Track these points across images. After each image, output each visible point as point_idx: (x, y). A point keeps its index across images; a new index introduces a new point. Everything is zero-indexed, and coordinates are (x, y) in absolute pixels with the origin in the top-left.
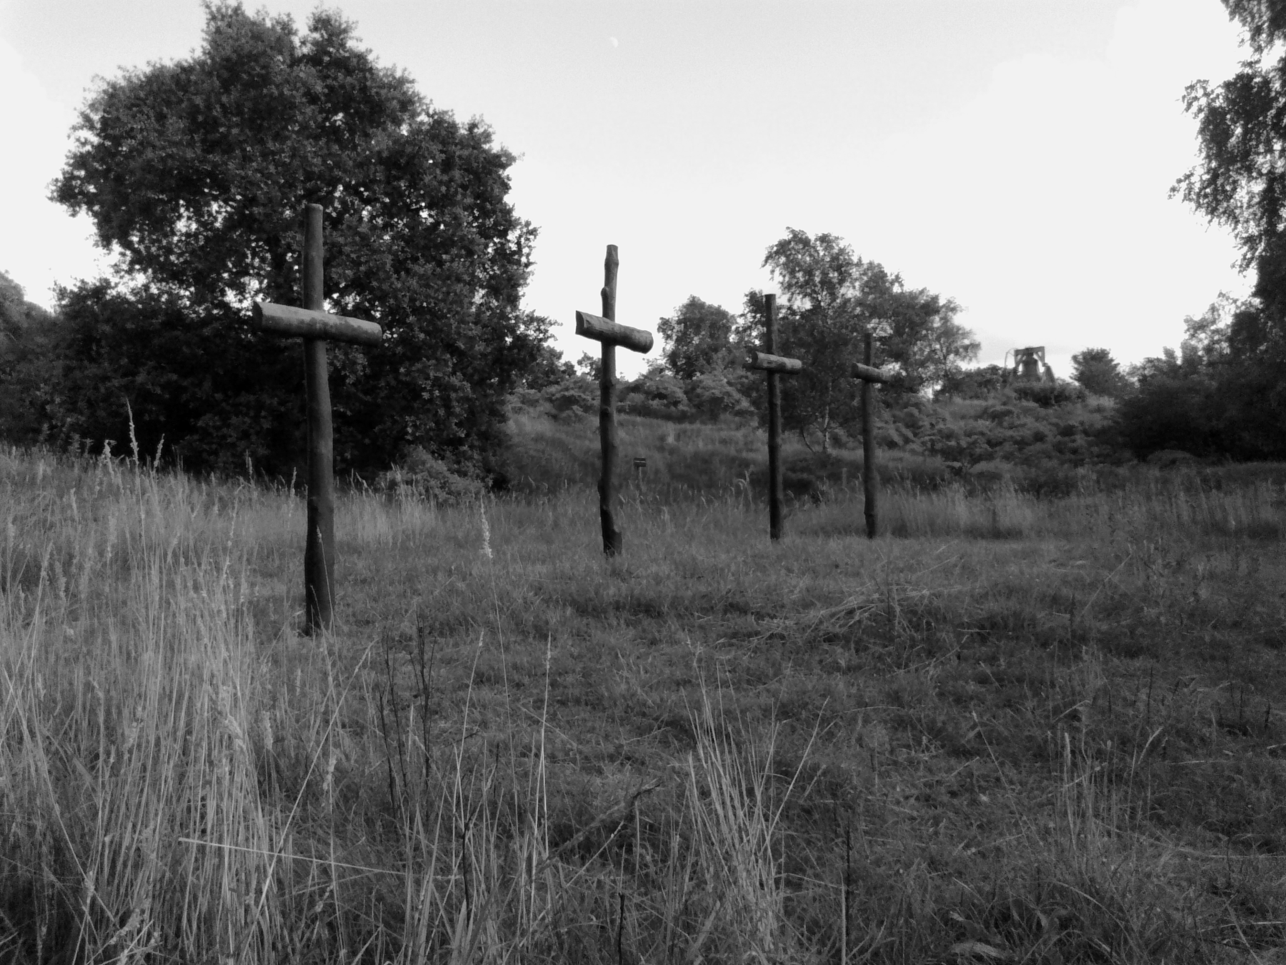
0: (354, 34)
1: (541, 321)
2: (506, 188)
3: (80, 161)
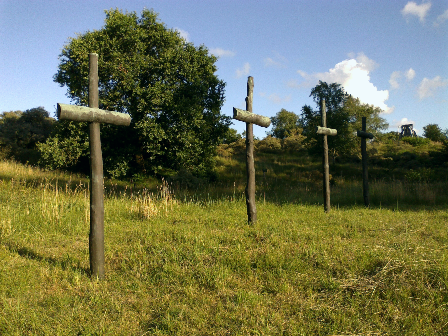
0: (158, 18)
1: (227, 118)
2: (214, 70)
3: (62, 67)
